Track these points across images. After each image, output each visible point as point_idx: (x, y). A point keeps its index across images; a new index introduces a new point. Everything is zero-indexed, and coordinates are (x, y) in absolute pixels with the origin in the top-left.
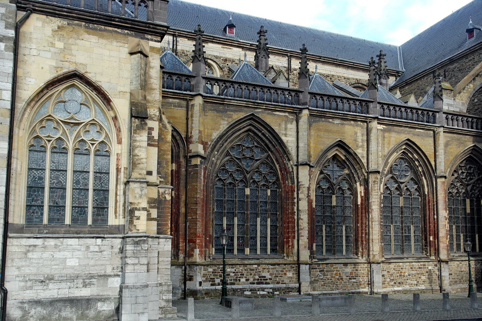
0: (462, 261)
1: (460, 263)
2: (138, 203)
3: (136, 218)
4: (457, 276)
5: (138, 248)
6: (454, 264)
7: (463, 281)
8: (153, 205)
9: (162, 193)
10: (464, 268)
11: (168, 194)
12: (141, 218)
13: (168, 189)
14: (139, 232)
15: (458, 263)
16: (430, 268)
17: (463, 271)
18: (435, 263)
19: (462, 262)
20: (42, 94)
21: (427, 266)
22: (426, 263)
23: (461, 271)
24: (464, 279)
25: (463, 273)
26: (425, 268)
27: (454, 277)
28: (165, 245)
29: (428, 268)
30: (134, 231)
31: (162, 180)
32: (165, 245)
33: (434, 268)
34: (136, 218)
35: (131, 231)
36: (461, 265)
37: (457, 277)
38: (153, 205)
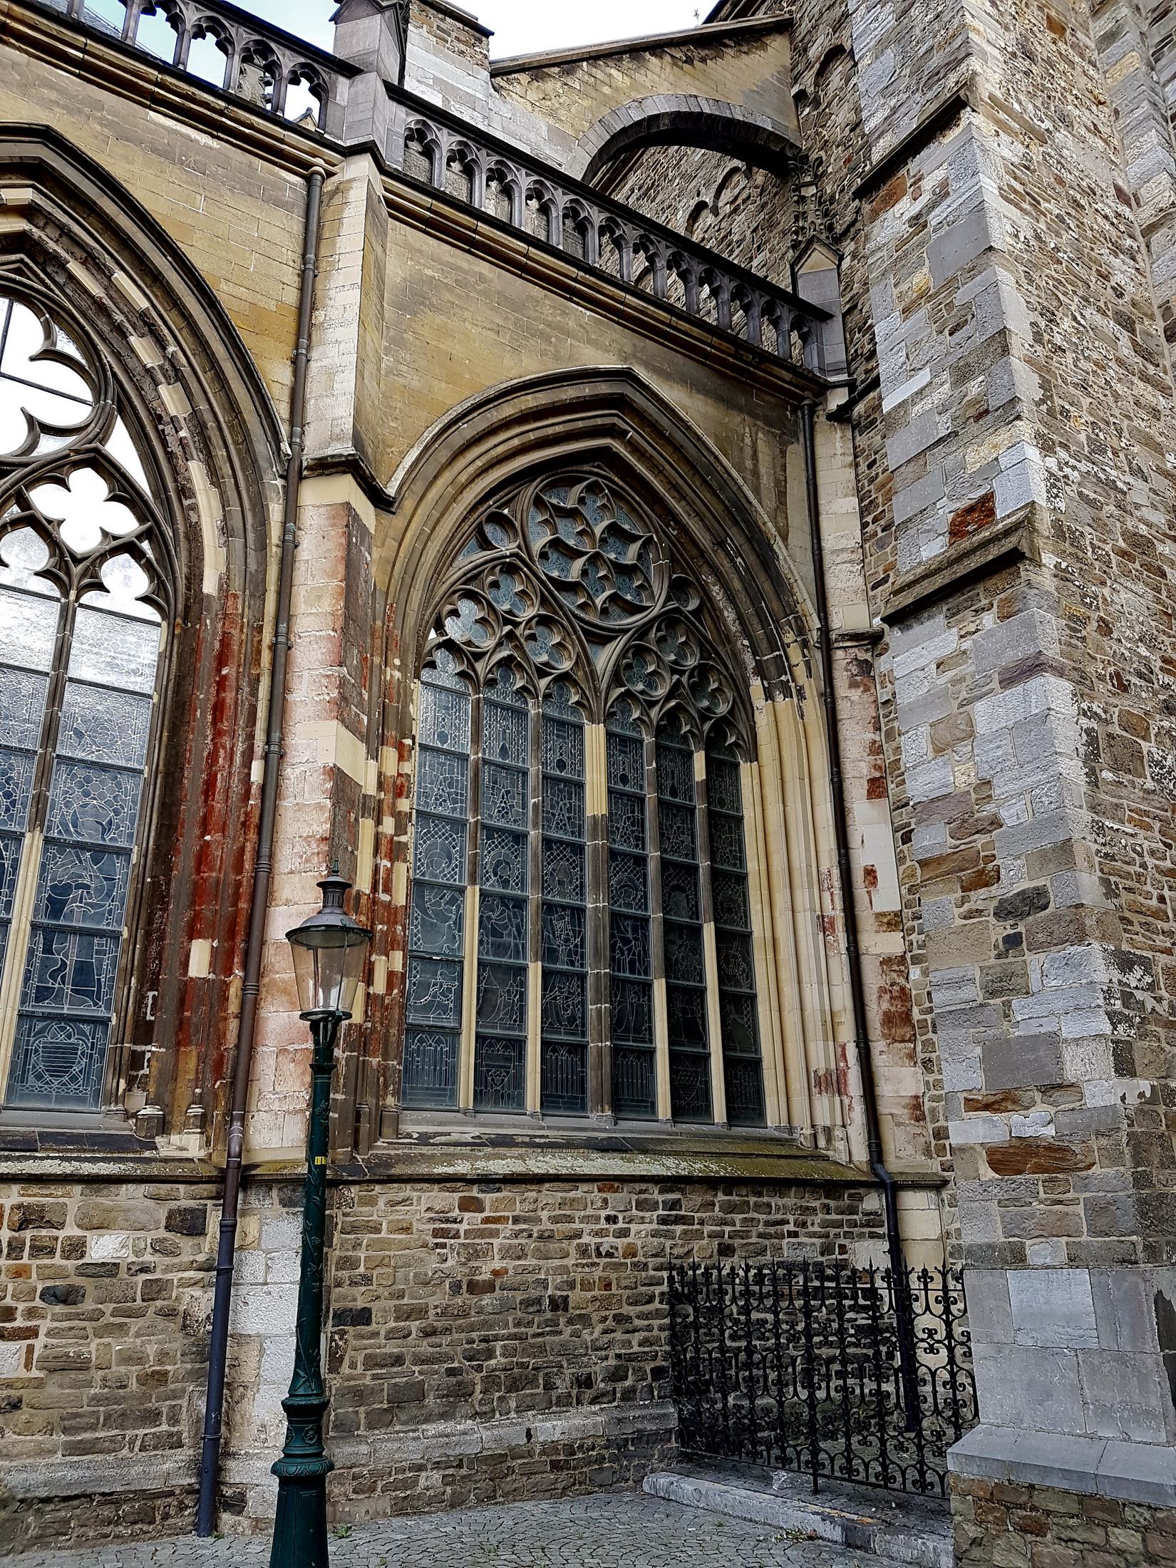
0: (486, 1181)
1: (469, 1205)
4: (428, 1333)
6: (400, 1214)
7: (491, 1382)
10: (506, 1253)
15: (447, 1199)
16: (103, 1248)
17: (489, 1287)
18: (184, 1198)
19: (488, 1198)
21: (71, 1231)
22: (74, 1198)
23: (474, 1287)
24: (498, 1361)
25: (487, 1300)
26: (40, 1250)
27: (392, 1348)
29: (76, 1248)
33: (159, 1248)
36: (471, 1220)
37: (425, 1348)
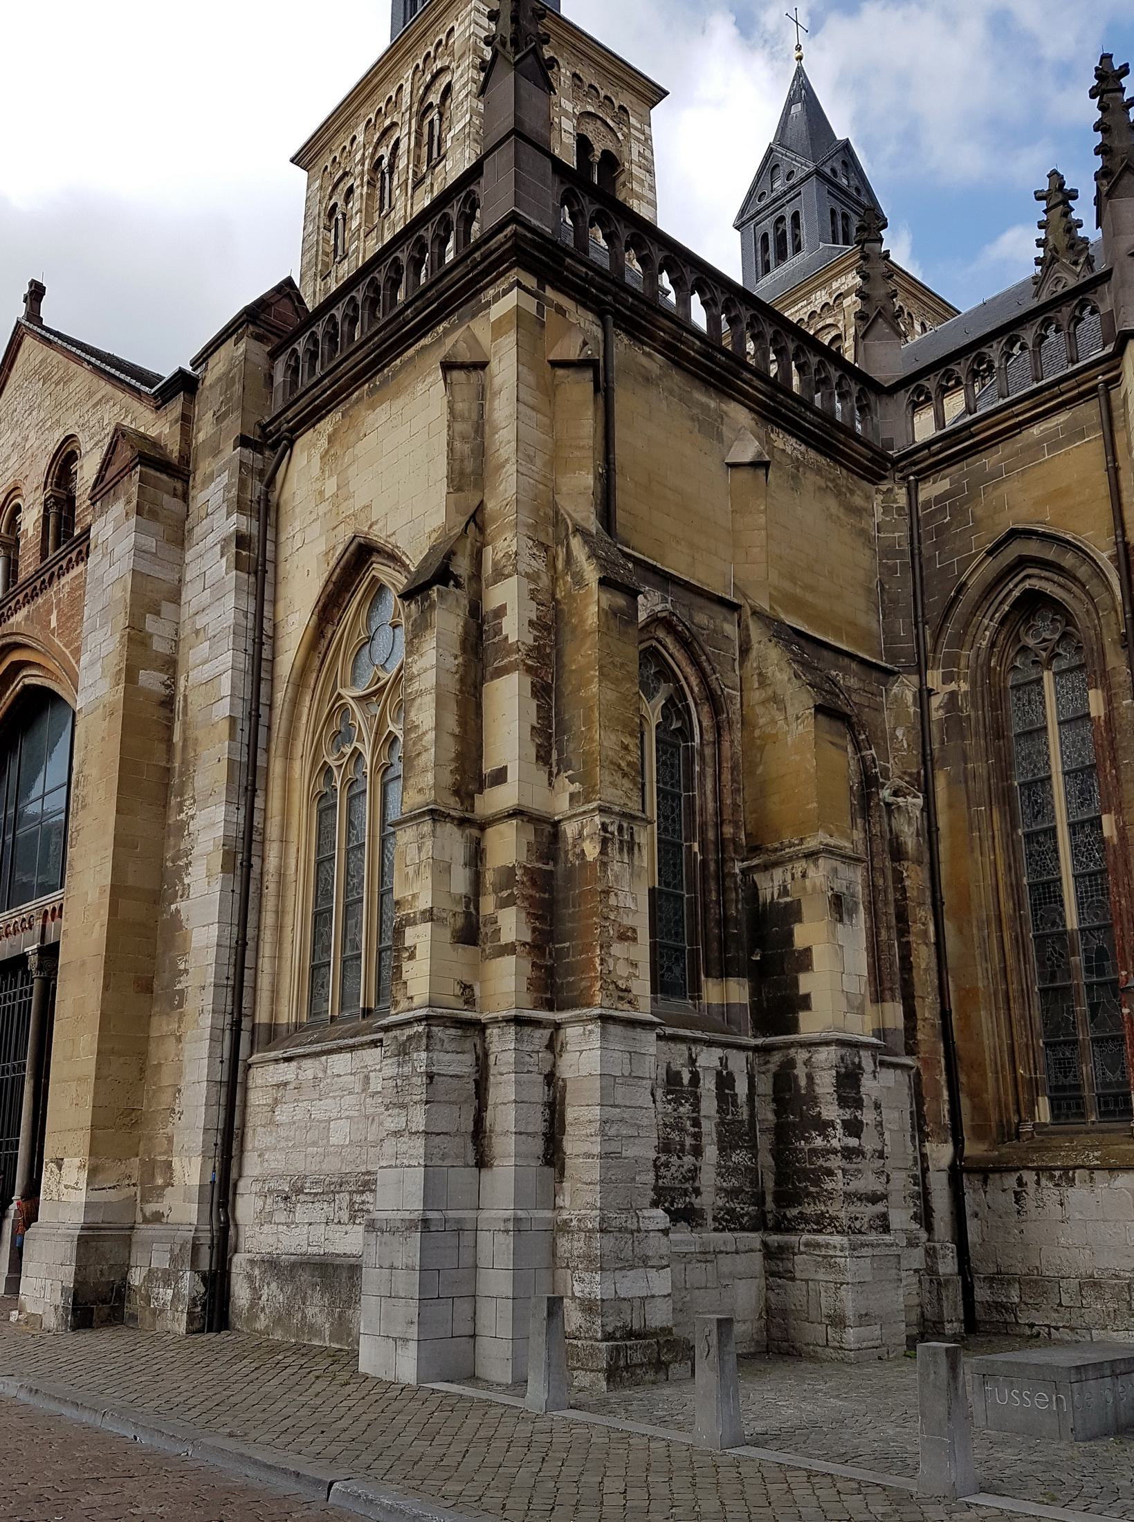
2: (414, 896)
3: (406, 955)
5: (407, 1069)
8: (505, 894)
9: (575, 839)
11: (591, 836)
12: (417, 952)
13: (587, 817)
14: (414, 1005)
20: (324, 643)
28: (581, 1052)
30: (404, 1004)
31: (576, 787)
32: (581, 1052)
34: (406, 955)
35: (396, 1004)
38: (505, 894)
